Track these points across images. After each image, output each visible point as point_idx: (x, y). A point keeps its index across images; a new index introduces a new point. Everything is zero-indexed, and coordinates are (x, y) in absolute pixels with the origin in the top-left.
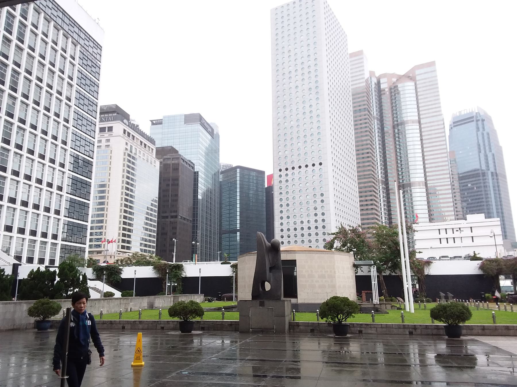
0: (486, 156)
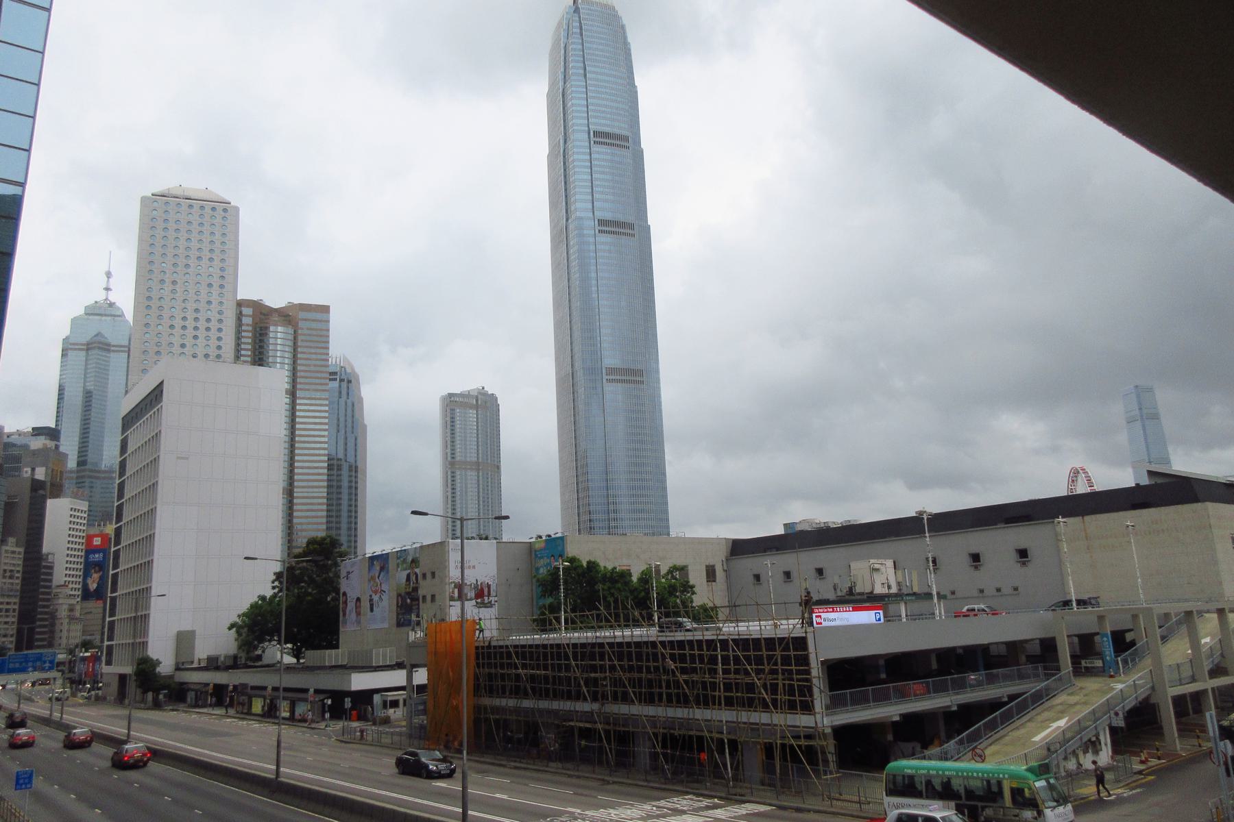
0: (346, 438)
